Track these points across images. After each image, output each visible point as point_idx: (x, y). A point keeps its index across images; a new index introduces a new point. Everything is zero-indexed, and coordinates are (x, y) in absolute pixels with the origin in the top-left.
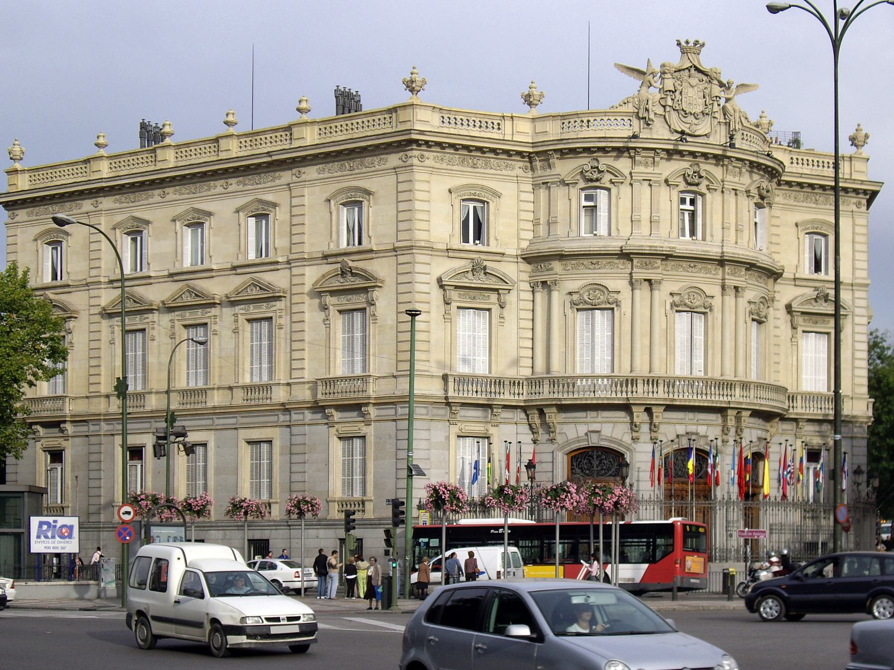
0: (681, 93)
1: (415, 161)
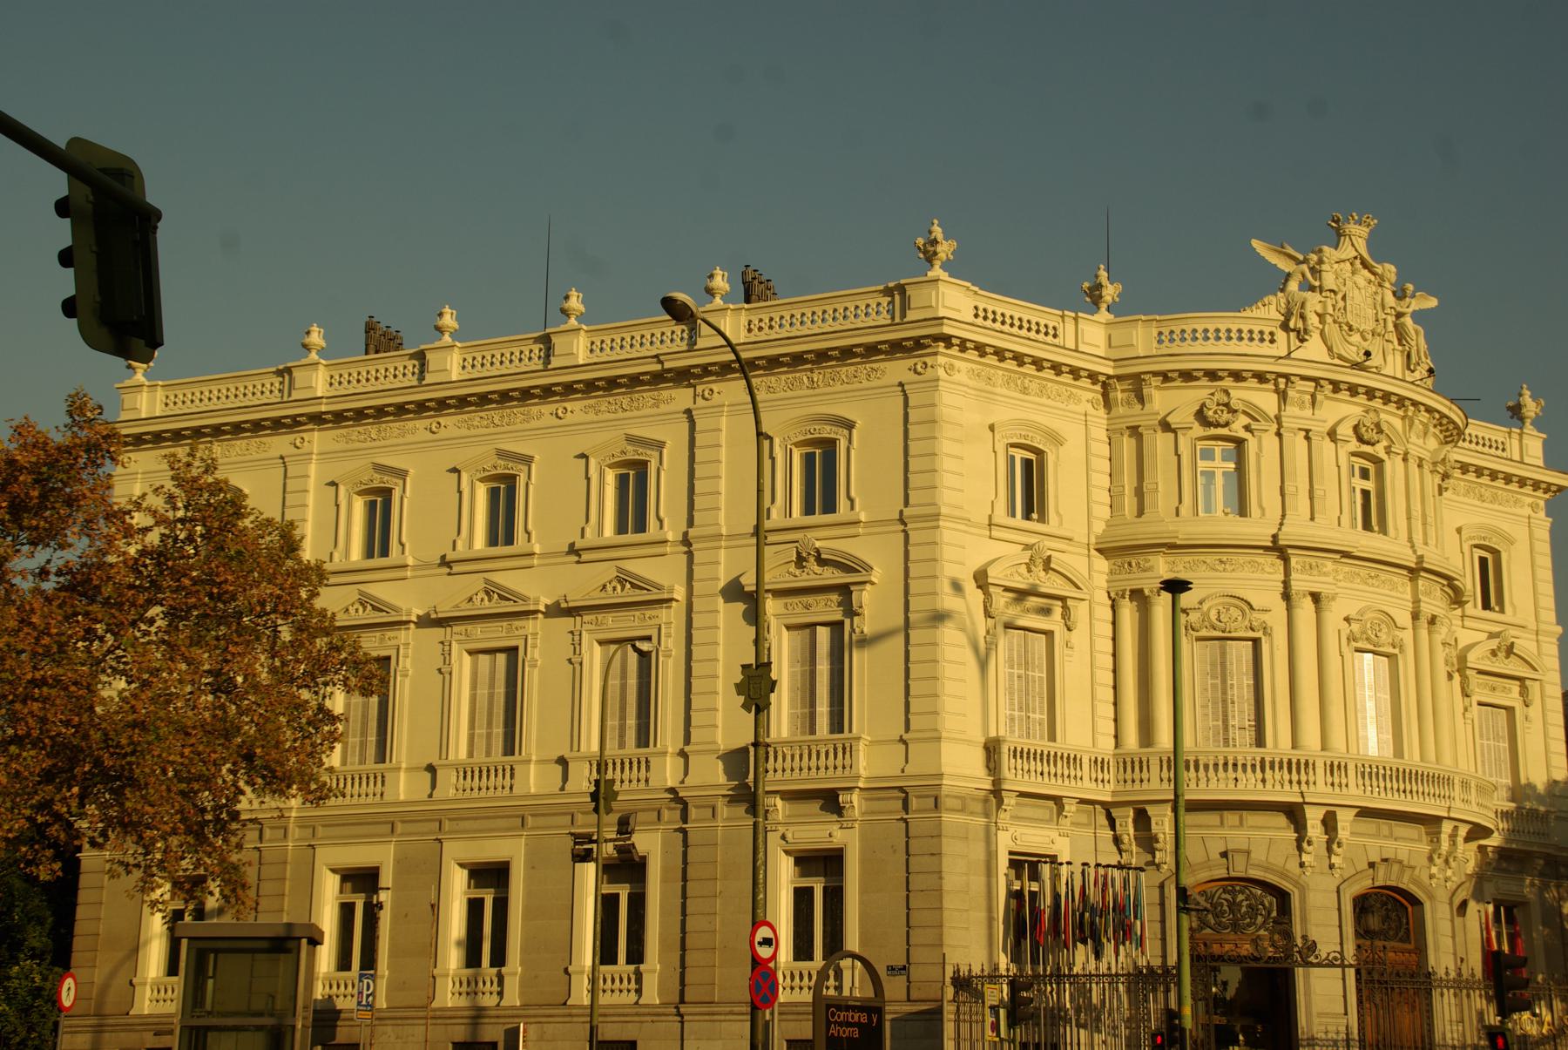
0: (1344, 298)
1: (941, 372)
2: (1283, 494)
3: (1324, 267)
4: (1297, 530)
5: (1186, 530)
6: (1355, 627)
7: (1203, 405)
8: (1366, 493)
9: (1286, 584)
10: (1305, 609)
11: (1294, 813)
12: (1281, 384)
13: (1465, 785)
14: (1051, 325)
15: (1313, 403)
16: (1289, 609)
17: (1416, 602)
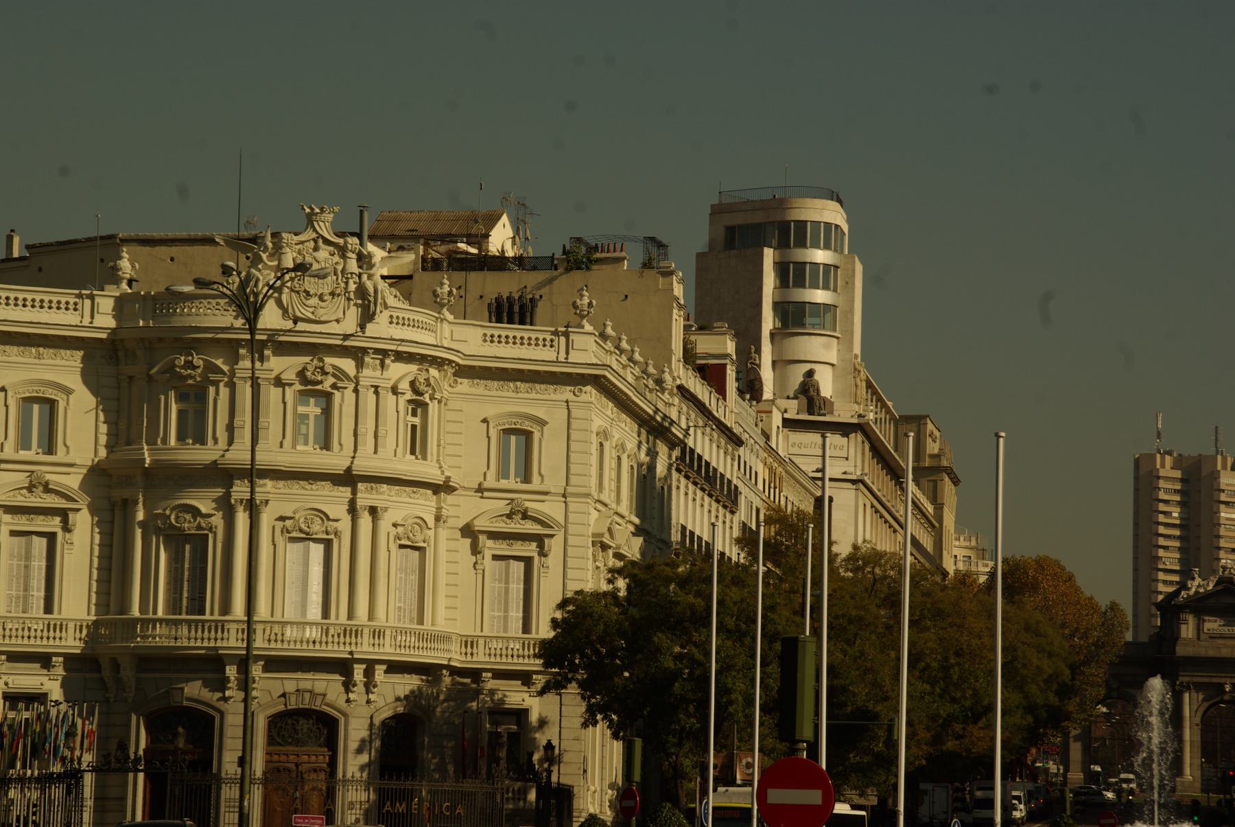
7: (305, 369)
10: (365, 521)
12: (358, 355)
15: (382, 365)
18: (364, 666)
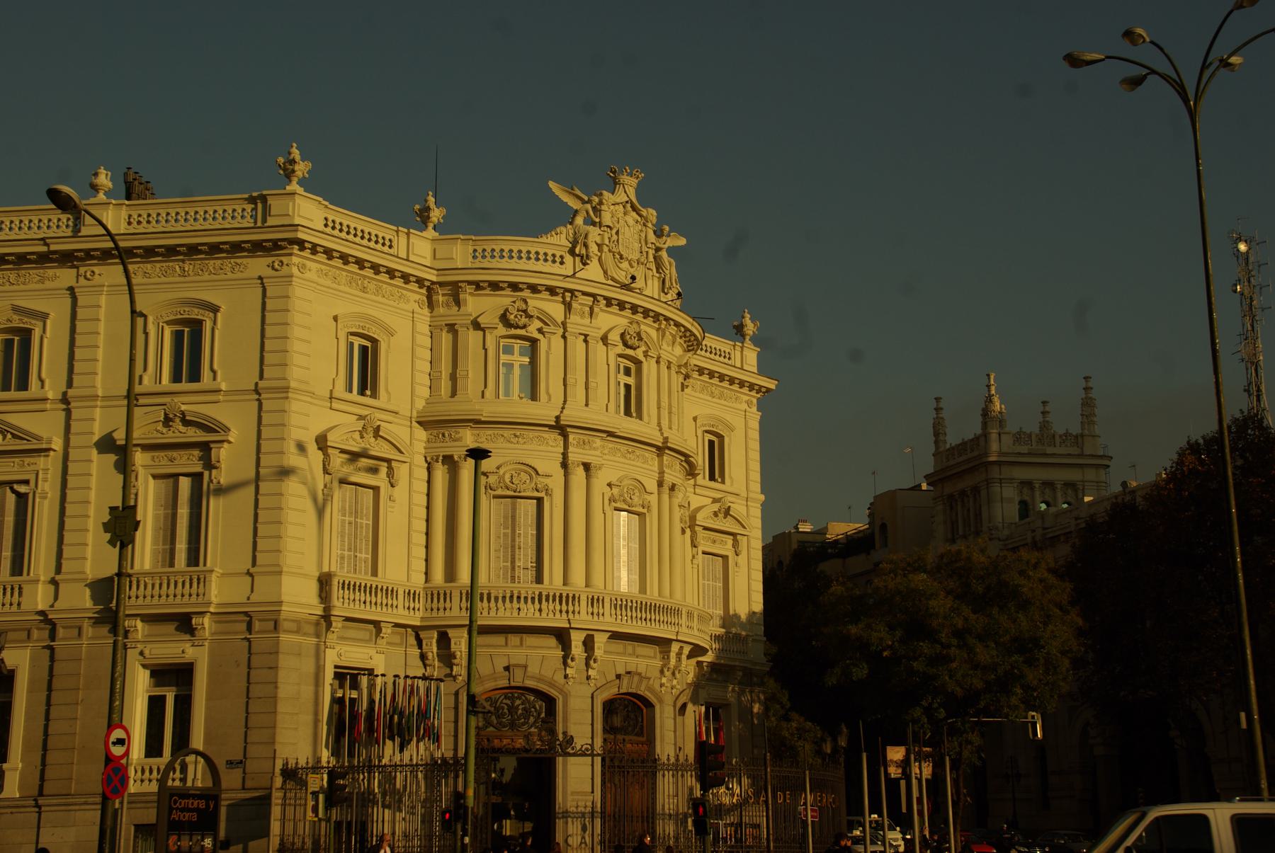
0: (617, 233)
1: (295, 270)
2: (565, 385)
3: (603, 207)
4: (575, 413)
5: (488, 410)
6: (615, 491)
7: (507, 310)
8: (628, 387)
9: (565, 455)
10: (578, 475)
11: (562, 636)
12: (567, 297)
13: (690, 615)
14: (387, 237)
16: (566, 475)
17: (662, 473)
18: (582, 636)
